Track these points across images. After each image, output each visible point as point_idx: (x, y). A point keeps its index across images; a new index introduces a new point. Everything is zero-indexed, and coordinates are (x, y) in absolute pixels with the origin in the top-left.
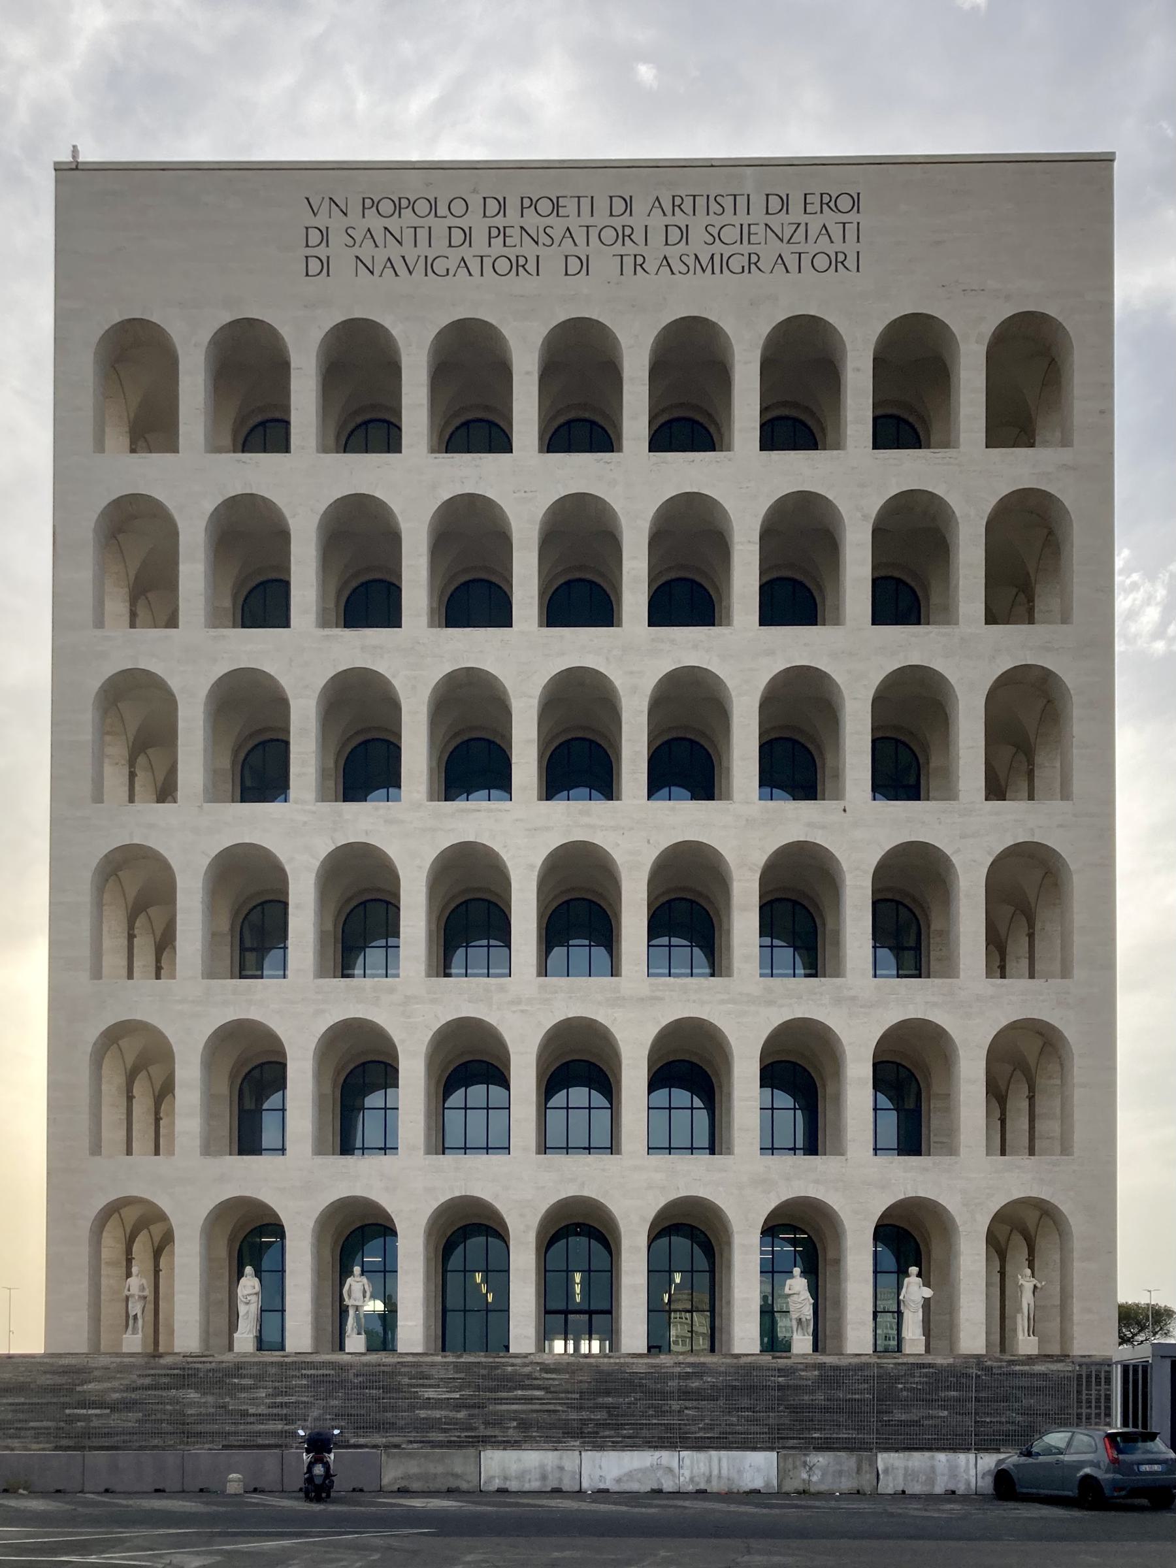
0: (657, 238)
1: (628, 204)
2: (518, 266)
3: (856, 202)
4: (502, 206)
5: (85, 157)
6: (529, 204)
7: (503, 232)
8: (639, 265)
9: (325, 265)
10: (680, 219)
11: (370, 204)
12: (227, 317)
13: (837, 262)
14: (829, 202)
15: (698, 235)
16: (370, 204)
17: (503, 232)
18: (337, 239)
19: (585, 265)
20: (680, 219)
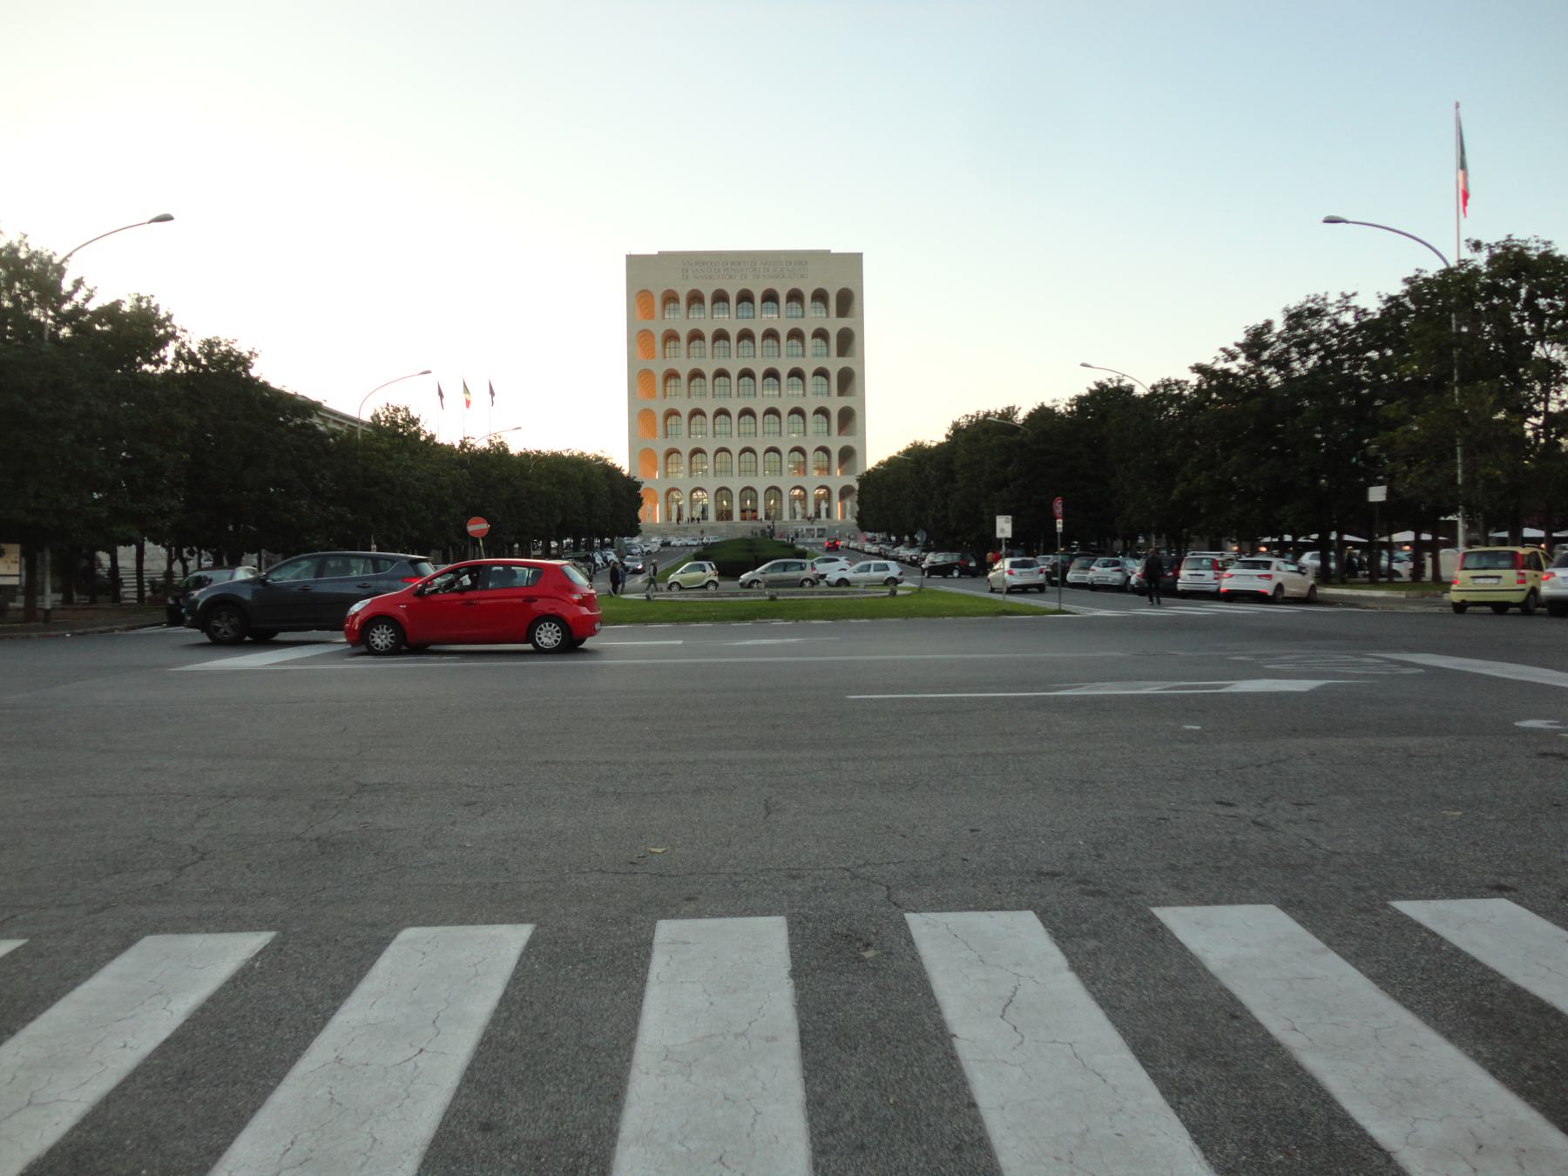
0: (762, 270)
1: (755, 264)
2: (731, 277)
3: (806, 263)
4: (727, 264)
5: (633, 253)
6: (733, 263)
7: (727, 269)
8: (758, 277)
9: (687, 277)
10: (767, 267)
11: (697, 263)
12: (665, 289)
13: (802, 276)
14: (800, 263)
15: (771, 270)
16: (697, 263)
17: (727, 269)
18: (690, 272)
19: (746, 277)
20: (767, 267)
